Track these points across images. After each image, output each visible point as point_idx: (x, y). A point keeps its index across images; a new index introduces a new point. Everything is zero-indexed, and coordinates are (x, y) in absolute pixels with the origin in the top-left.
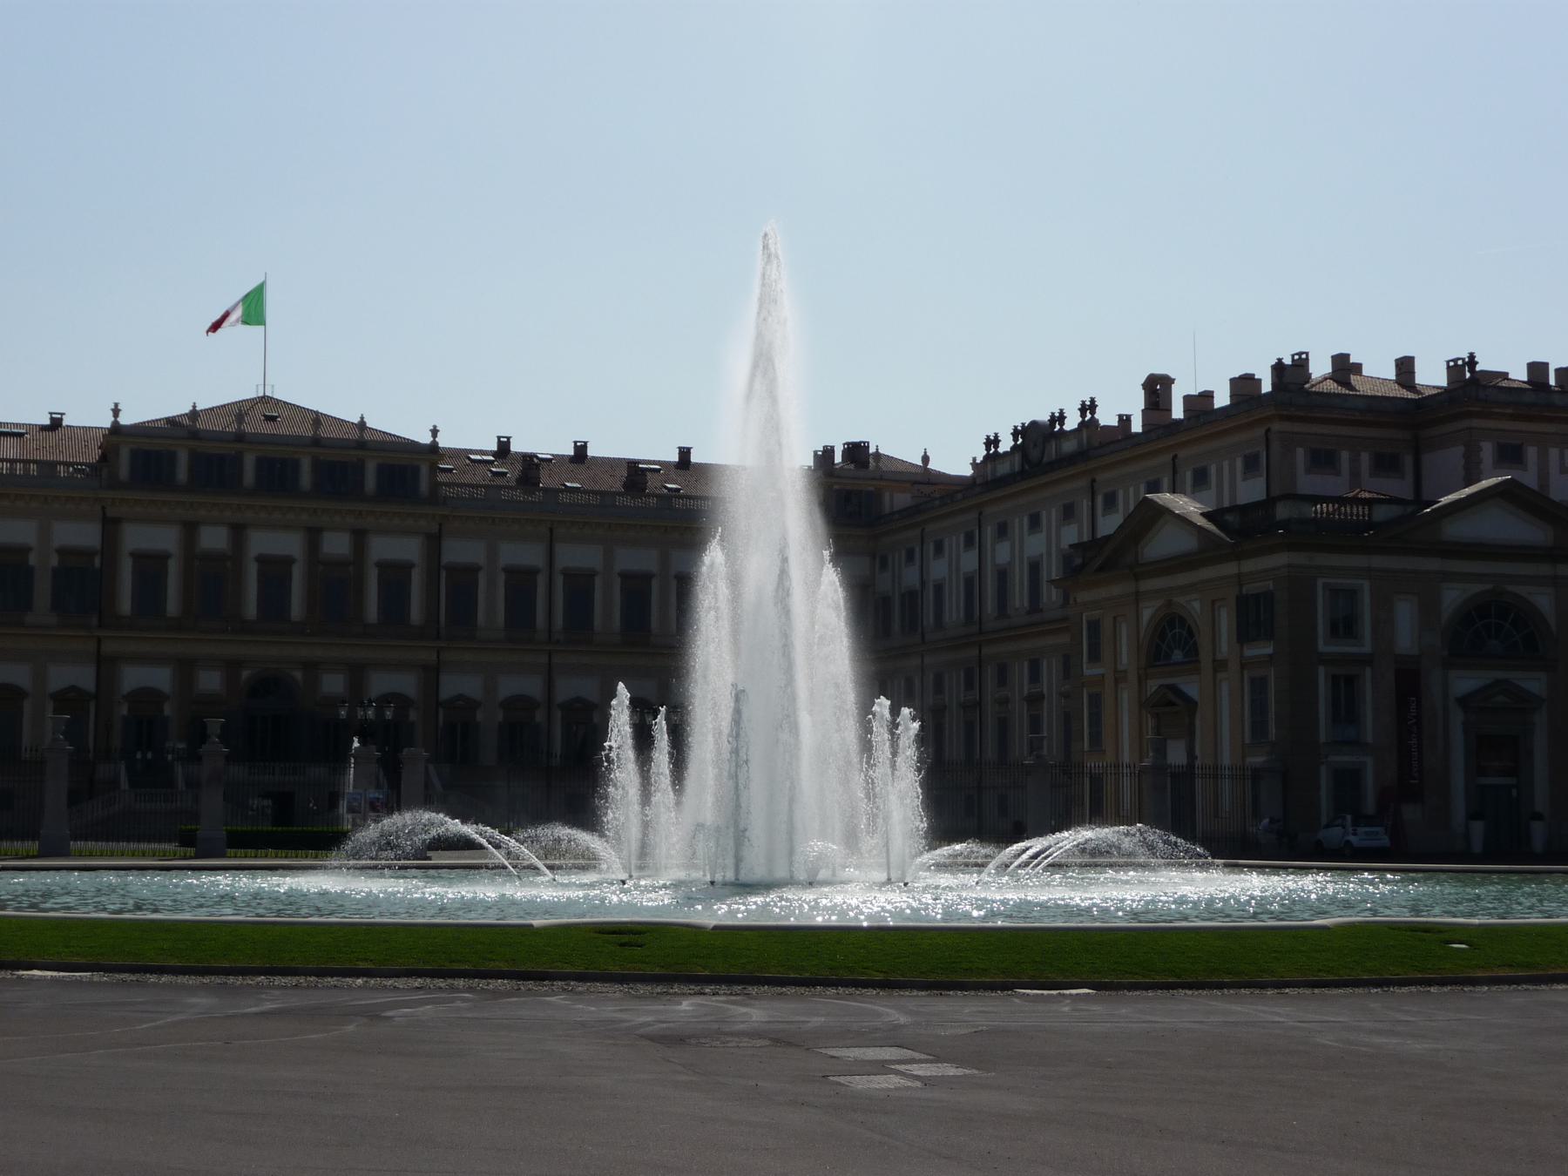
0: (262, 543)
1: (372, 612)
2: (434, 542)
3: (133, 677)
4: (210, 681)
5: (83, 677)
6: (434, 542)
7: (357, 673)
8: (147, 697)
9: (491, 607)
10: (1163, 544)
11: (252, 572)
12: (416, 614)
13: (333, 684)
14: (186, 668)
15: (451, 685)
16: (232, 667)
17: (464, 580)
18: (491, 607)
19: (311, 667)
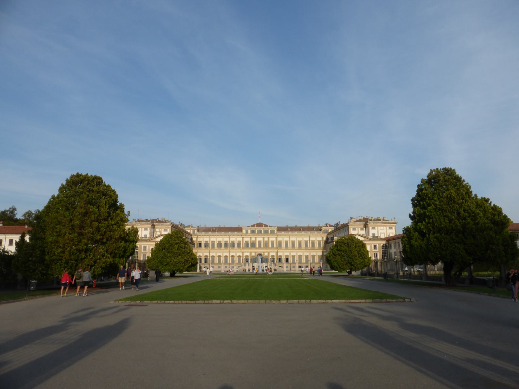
0: (258, 239)
1: (270, 246)
2: (277, 238)
3: (245, 254)
4: (253, 254)
5: (241, 254)
6: (277, 238)
7: (269, 253)
8: (247, 256)
9: (283, 245)
10: (330, 241)
11: (257, 242)
12: (275, 246)
13: (266, 254)
14: (251, 253)
15: (279, 254)
16: (256, 252)
17: (280, 243)
18: (283, 245)
19: (264, 252)
